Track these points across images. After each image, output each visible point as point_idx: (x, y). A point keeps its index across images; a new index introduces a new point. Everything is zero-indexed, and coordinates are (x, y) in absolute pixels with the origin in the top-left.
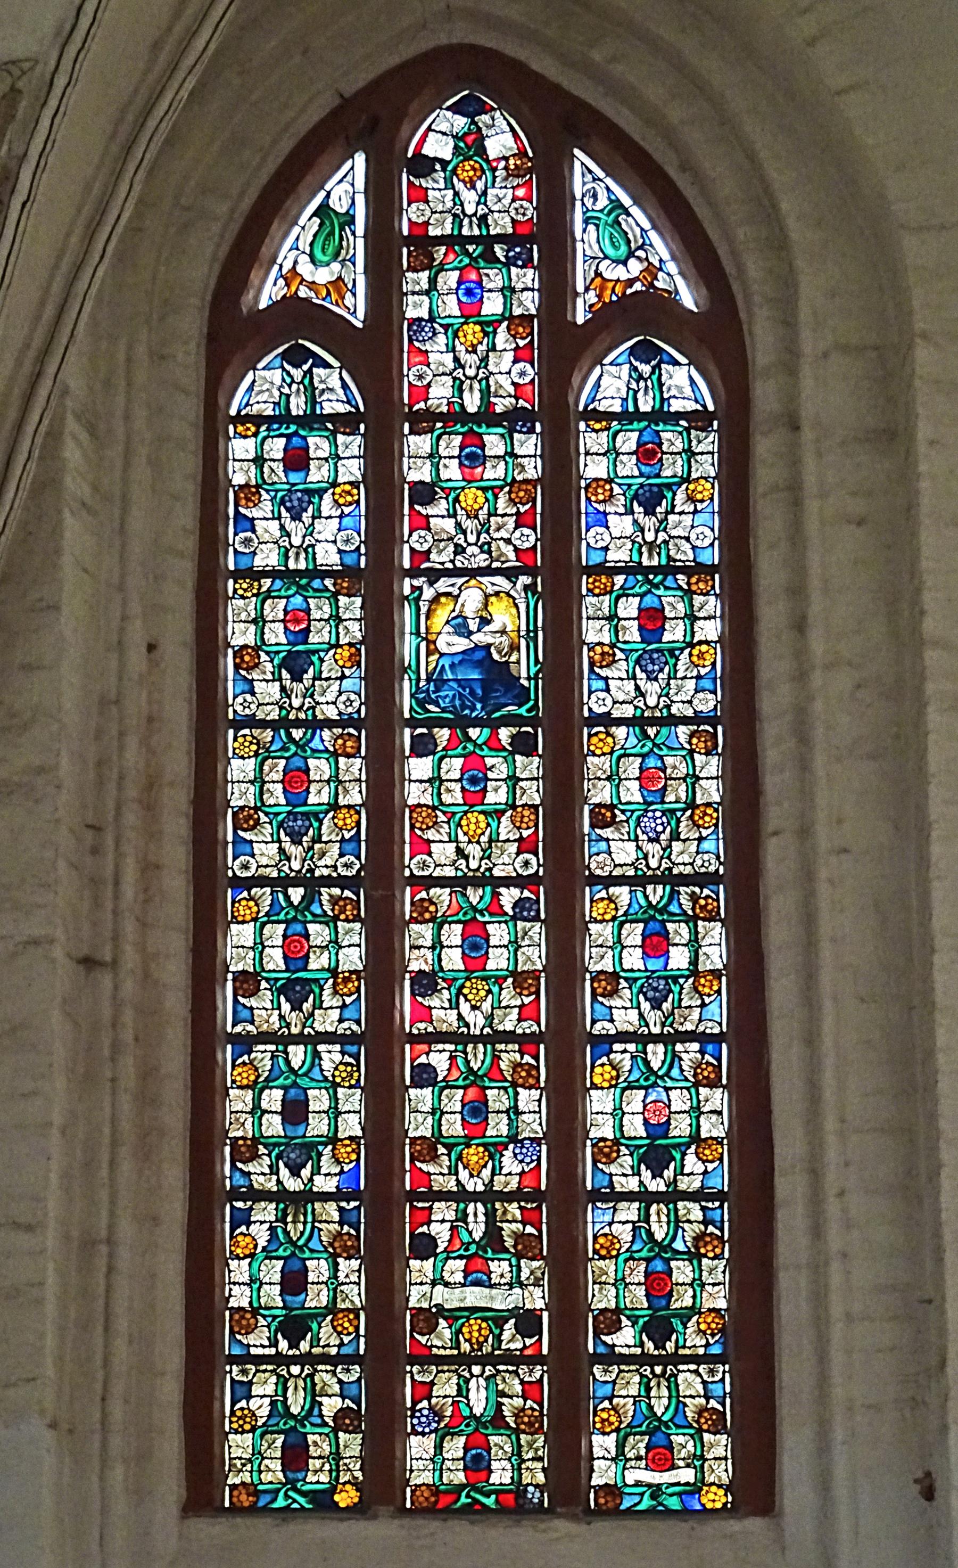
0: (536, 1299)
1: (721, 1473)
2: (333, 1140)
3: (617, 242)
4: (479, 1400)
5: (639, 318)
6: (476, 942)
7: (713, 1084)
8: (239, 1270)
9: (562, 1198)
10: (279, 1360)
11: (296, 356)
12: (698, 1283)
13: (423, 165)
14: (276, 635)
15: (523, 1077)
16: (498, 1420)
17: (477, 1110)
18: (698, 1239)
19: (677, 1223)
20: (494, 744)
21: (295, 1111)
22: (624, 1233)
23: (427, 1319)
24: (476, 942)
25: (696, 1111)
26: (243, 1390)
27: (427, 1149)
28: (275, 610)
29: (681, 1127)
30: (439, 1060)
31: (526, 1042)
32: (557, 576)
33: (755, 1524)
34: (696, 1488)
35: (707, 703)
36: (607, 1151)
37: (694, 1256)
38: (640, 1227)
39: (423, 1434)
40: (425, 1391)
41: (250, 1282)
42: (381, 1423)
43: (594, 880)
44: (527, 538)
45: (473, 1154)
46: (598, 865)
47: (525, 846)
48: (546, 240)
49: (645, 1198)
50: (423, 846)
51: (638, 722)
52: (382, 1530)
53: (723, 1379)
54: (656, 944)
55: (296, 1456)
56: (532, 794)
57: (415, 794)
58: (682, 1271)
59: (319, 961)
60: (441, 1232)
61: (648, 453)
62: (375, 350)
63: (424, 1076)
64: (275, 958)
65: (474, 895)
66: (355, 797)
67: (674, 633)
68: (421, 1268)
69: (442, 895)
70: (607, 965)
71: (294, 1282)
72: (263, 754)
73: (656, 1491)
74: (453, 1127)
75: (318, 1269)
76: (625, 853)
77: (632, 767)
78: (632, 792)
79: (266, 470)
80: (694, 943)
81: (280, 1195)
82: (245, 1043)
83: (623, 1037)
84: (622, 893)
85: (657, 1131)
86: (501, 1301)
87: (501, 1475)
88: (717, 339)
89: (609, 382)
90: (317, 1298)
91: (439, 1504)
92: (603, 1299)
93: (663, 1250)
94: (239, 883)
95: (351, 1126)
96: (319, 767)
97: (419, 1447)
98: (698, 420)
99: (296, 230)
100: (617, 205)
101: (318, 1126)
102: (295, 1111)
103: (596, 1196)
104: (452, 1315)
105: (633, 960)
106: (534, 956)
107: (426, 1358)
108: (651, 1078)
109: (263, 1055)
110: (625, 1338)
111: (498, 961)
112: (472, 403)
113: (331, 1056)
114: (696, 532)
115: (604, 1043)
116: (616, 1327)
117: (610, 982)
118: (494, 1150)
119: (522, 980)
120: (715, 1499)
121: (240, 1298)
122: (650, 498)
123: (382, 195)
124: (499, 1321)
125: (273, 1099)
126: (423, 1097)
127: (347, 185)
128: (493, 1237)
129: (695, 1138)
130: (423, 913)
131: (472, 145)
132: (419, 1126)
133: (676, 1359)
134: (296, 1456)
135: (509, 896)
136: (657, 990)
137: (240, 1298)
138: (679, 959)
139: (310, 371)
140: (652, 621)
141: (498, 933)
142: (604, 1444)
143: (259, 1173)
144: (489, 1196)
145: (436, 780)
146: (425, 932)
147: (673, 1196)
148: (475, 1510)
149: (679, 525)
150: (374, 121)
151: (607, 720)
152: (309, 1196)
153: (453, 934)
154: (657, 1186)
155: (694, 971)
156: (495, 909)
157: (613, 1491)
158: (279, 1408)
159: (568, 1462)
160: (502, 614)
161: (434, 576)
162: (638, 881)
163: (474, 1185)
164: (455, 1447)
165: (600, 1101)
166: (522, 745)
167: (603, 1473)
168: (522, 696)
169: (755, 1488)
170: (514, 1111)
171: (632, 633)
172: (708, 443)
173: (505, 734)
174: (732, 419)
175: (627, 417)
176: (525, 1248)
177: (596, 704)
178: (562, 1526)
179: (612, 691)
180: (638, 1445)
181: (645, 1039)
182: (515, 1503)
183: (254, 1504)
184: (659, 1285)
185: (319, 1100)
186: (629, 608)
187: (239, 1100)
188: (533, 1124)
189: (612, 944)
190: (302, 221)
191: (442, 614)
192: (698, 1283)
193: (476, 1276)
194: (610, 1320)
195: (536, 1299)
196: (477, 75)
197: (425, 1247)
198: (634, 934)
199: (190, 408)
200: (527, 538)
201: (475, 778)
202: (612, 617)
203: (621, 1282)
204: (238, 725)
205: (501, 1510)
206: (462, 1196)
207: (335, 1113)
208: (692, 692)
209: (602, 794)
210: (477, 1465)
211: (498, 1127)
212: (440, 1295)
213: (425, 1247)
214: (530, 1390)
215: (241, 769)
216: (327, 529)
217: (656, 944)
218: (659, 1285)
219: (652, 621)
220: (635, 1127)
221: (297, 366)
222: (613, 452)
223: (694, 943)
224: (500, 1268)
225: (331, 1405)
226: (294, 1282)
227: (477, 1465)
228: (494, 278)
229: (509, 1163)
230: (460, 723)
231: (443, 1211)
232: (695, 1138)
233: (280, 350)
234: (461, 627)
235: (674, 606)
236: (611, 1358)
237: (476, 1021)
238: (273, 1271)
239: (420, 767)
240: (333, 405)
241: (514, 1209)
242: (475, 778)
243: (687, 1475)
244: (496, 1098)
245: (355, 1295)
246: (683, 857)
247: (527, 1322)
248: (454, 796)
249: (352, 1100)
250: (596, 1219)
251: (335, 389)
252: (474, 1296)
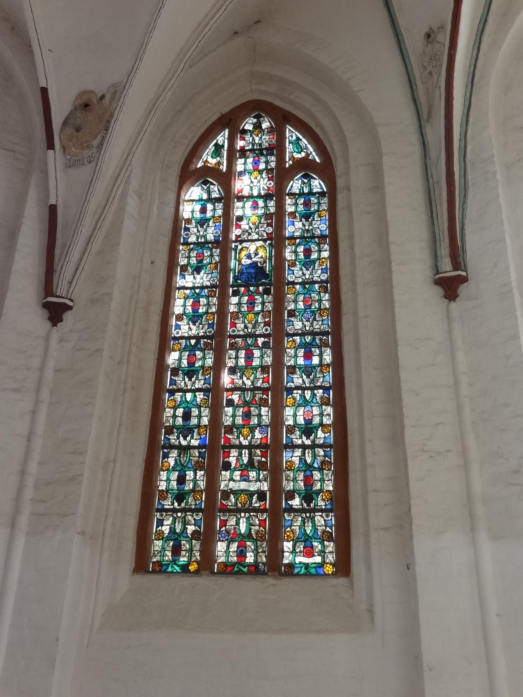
0: (265, 486)
1: (331, 558)
2: (198, 426)
3: (297, 146)
4: (243, 528)
5: (304, 167)
6: (249, 357)
7: (327, 404)
8: (164, 475)
9: (275, 447)
10: (175, 511)
11: (206, 182)
12: (322, 480)
13: (244, 132)
14: (193, 261)
15: (264, 403)
16: (249, 536)
17: (247, 415)
18: (323, 462)
19: (315, 456)
20: (257, 292)
21: (187, 416)
22: (296, 460)
23: (226, 494)
24: (249, 357)
25: (321, 415)
26: (160, 523)
27: (229, 429)
28: (194, 254)
29: (316, 421)
30: (235, 397)
31: (265, 391)
32: (277, 240)
33: (342, 581)
34: (321, 565)
35: (324, 277)
36: (291, 430)
37: (321, 469)
38: (302, 459)
39: (223, 541)
40: (224, 523)
41: (166, 480)
42: (207, 538)
43: (289, 335)
44: (270, 230)
45: (245, 431)
46: (290, 330)
47: (267, 324)
48: (277, 149)
49: (304, 447)
50: (234, 325)
51: (303, 284)
52: (205, 581)
53: (332, 518)
54: (308, 356)
55: (176, 551)
56: (269, 307)
57: (232, 309)
58: (317, 475)
59: (198, 364)
60: (233, 460)
61: (307, 204)
62: (226, 179)
63: (230, 403)
64: (185, 363)
65: (249, 341)
66: (214, 310)
67: (314, 256)
68: (226, 474)
69: (239, 340)
70: (292, 363)
71: (181, 480)
72: (186, 298)
73: (307, 566)
74: (239, 421)
75: (190, 475)
76: (298, 325)
77: (301, 297)
78: (301, 305)
79: (194, 214)
80: (321, 355)
81: (180, 447)
82: (172, 392)
83: (297, 388)
84: (298, 339)
85: (309, 422)
86: (253, 487)
87: (250, 558)
88: (326, 170)
89: (296, 185)
90: (189, 486)
91: (227, 570)
92: (289, 486)
93: (309, 467)
94: (176, 339)
95: (205, 421)
96: (203, 301)
97: (221, 546)
98: (322, 194)
99: (208, 150)
100: (298, 139)
101: (194, 421)
102: (187, 416)
103: (287, 447)
104: (236, 493)
105: (301, 361)
106: (268, 360)
107: (224, 510)
108: (305, 403)
109: (178, 396)
110: (296, 502)
111: (256, 362)
112: (255, 193)
113: (200, 396)
114: (321, 226)
115: (290, 391)
116: (293, 498)
117: (292, 370)
118: (252, 430)
119: (264, 369)
120: (329, 569)
121: (163, 486)
122: (307, 217)
123: (232, 140)
124: (251, 494)
125: (180, 412)
126: (229, 410)
127: (223, 138)
128: (251, 463)
129: (321, 424)
130: (233, 346)
131: (258, 126)
132: (227, 421)
133: (315, 510)
134: (176, 551)
135: (260, 341)
136: (308, 370)
137: (163, 486)
138: (316, 360)
139: (209, 187)
140: (308, 252)
141: (257, 353)
142: (288, 546)
143: (173, 439)
144: (250, 447)
145: (239, 304)
146: (233, 353)
147: (314, 446)
148: (240, 573)
149: (316, 224)
150: (230, 121)
151: (293, 283)
152: (189, 447)
153: (242, 354)
154: (308, 442)
155: (321, 365)
156: (256, 345)
157: (291, 566)
158: (172, 530)
159: (275, 553)
160: (261, 253)
161: (241, 242)
162: (303, 335)
163: (245, 443)
164: (234, 547)
165: (289, 412)
166: (267, 292)
167: (288, 558)
168: (267, 276)
169: (343, 566)
170: (259, 416)
171: (302, 256)
172: (325, 200)
173: (261, 288)
174: (331, 193)
175: (301, 194)
176: (262, 466)
177: (291, 278)
178: (269, 580)
179: (295, 274)
180: (300, 547)
181: (303, 389)
182: (255, 570)
183: (160, 568)
184: (308, 481)
185: (195, 412)
186: (301, 249)
187: (169, 412)
188: (266, 420)
189: (294, 357)
190: (210, 148)
191: (244, 253)
192: (322, 480)
193: (245, 478)
194: (291, 495)
195: (265, 486)
196: (258, 108)
197: (227, 466)
198: (301, 352)
199: (172, 196)
200: (270, 230)
201: (251, 303)
202: (295, 252)
203: (295, 480)
204: (180, 288)
205: (249, 573)
206: (240, 447)
207: (200, 417)
208: (319, 274)
209: (292, 306)
210: (241, 554)
211: (255, 421)
212: (232, 485)
213: (227, 466)
214: (262, 523)
215: (179, 302)
216: (211, 230)
217: (308, 356)
218: (308, 481)
219: (308, 252)
220: (301, 420)
221: (205, 185)
222: (296, 204)
223: (321, 355)
224: (253, 474)
225: (191, 529)
226: (181, 480)
227: (241, 554)
228: (263, 159)
229: (258, 435)
230: (247, 286)
231: (234, 453)
232: (321, 424)
233: (201, 181)
234: (249, 257)
235: (314, 247)
236: (290, 510)
237: (248, 383)
238: (175, 476)
239: (235, 300)
240: (215, 195)
241: (258, 452)
242: (251, 303)
243: (318, 559)
244: (254, 410)
245: (202, 485)
246: (317, 326)
247: (261, 496)
248: (245, 308)
249: (206, 412)
250: (286, 455)
251: (216, 191)
252: (243, 485)
